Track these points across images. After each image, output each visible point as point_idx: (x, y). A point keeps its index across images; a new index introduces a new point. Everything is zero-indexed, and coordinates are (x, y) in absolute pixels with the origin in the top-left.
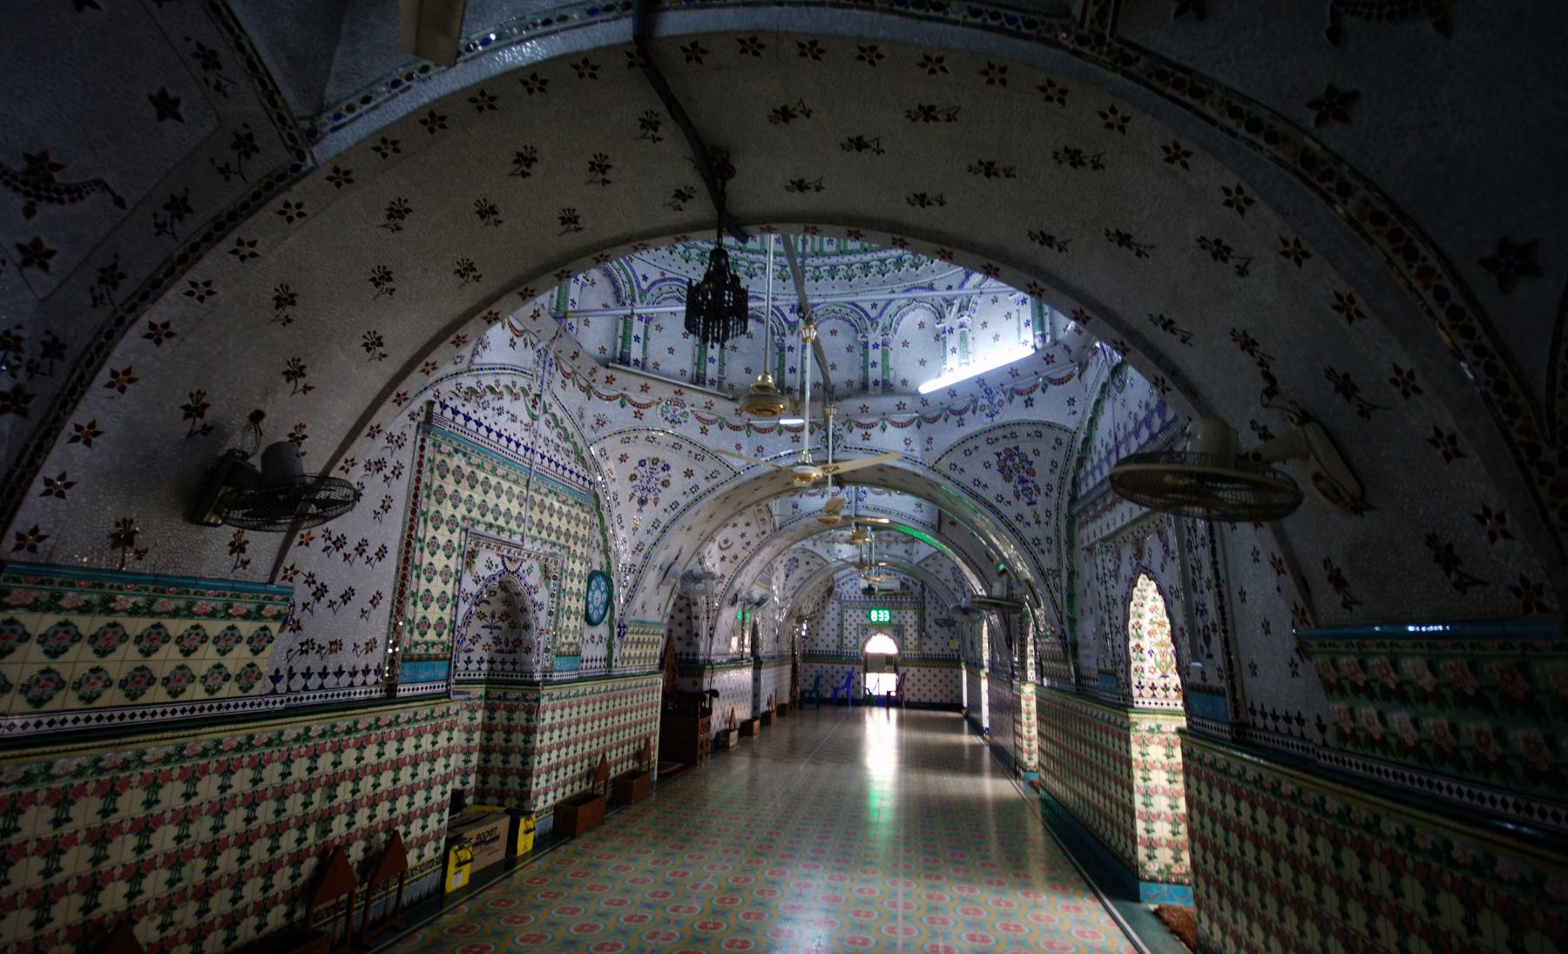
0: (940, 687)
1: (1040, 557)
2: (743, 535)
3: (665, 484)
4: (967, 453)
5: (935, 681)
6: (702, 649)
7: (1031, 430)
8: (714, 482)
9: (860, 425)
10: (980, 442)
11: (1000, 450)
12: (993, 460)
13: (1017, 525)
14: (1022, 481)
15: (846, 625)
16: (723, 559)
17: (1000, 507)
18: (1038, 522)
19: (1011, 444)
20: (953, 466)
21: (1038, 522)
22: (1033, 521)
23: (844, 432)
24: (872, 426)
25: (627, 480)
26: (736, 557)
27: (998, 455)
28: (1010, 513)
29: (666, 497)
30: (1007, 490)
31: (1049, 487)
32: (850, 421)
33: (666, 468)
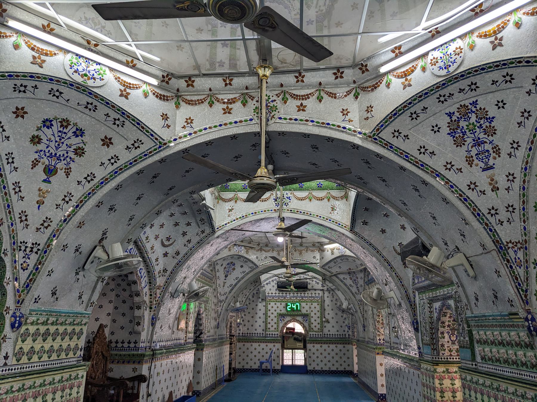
0: (337, 358)
1: (498, 228)
2: (184, 234)
3: (79, 152)
4: (414, 116)
5: (333, 354)
6: (144, 336)
7: (497, 75)
8: (136, 153)
9: (295, 97)
10: (431, 102)
11: (453, 109)
12: (443, 122)
13: (472, 195)
14: (478, 143)
15: (269, 313)
16: (166, 255)
17: (450, 175)
18: (495, 189)
19: (467, 99)
20: (397, 133)
21: (495, 189)
22: (488, 189)
23: (279, 103)
24: (307, 97)
25: (28, 143)
26: (178, 253)
27: (450, 115)
28: (461, 181)
29: (80, 168)
30: (458, 156)
31: (515, 145)
32: (284, 92)
33: (79, 133)
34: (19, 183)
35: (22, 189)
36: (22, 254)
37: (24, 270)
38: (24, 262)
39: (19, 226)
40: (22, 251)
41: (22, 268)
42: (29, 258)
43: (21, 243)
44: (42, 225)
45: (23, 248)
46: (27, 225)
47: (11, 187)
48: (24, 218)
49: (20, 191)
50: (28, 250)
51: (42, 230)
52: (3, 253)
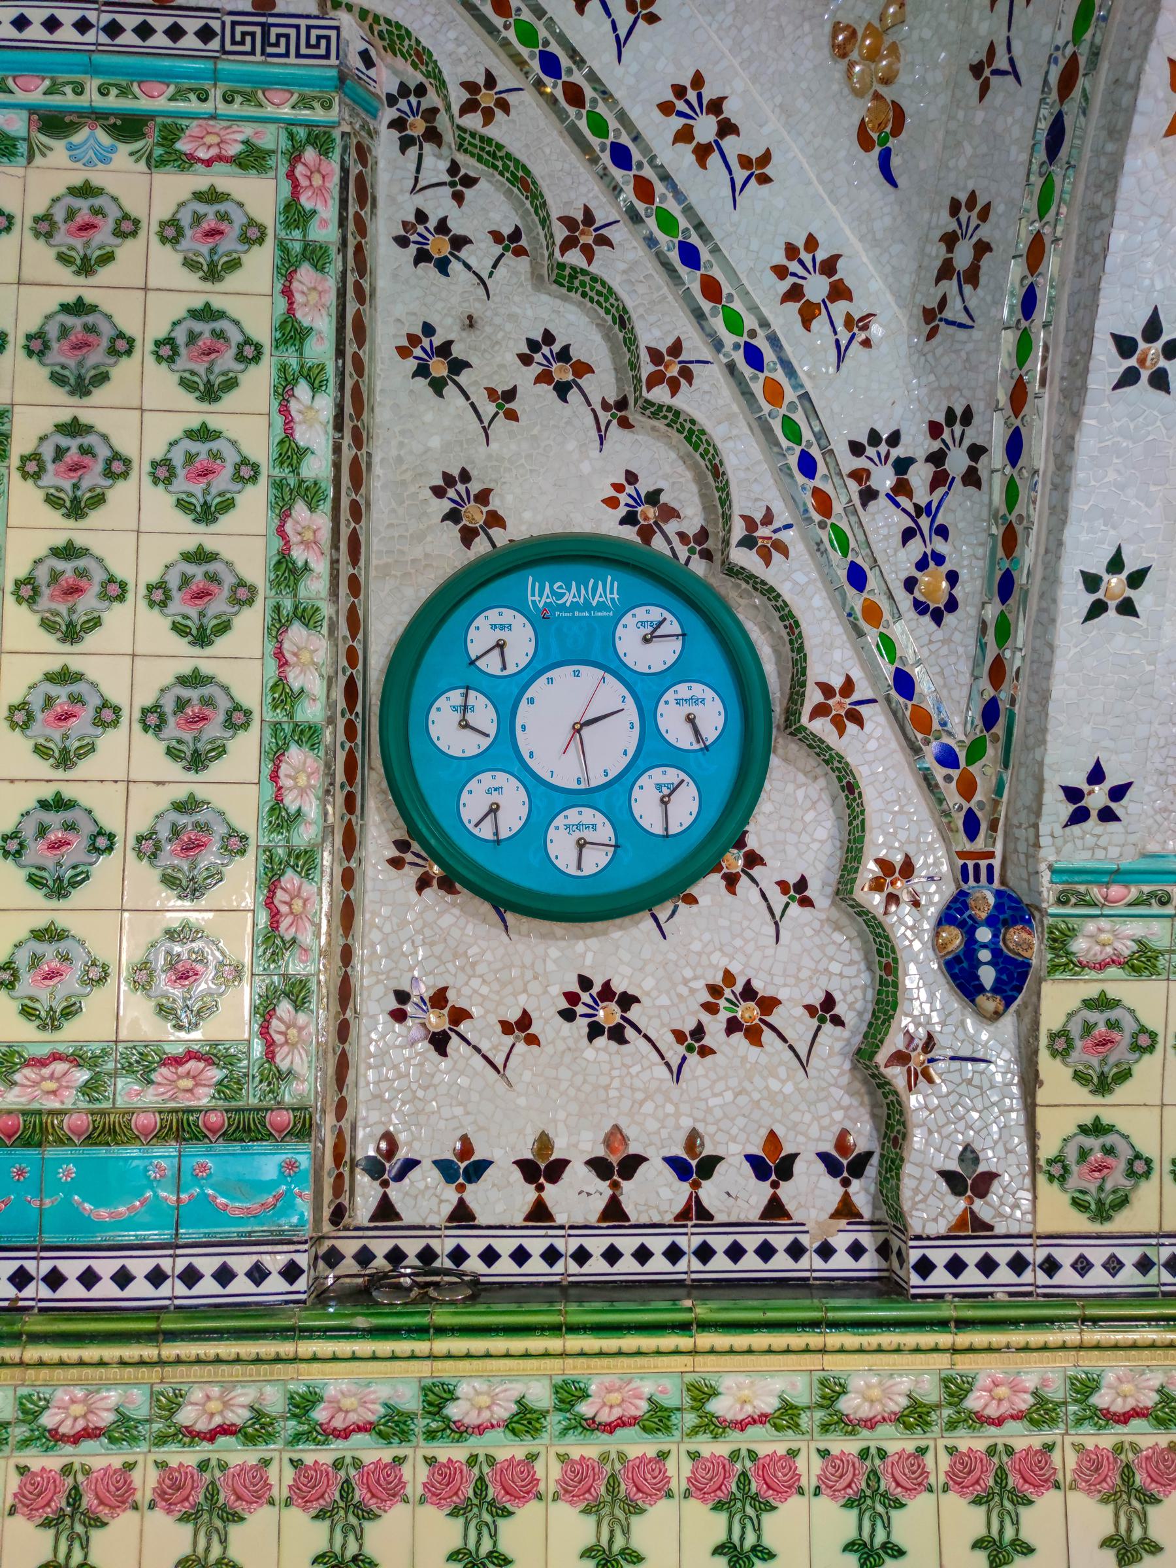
34: (698, 81)
35: (730, 110)
36: (884, 522)
37: (937, 617)
38: (922, 565)
39: (808, 349)
40: (882, 501)
41: (920, 607)
42: (943, 532)
43: (856, 449)
44: (946, 271)
45: (884, 479)
46: (858, 324)
47: (658, 132)
48: (816, 288)
49: (727, 128)
50: (919, 476)
51: (954, 310)
52: (748, 542)
